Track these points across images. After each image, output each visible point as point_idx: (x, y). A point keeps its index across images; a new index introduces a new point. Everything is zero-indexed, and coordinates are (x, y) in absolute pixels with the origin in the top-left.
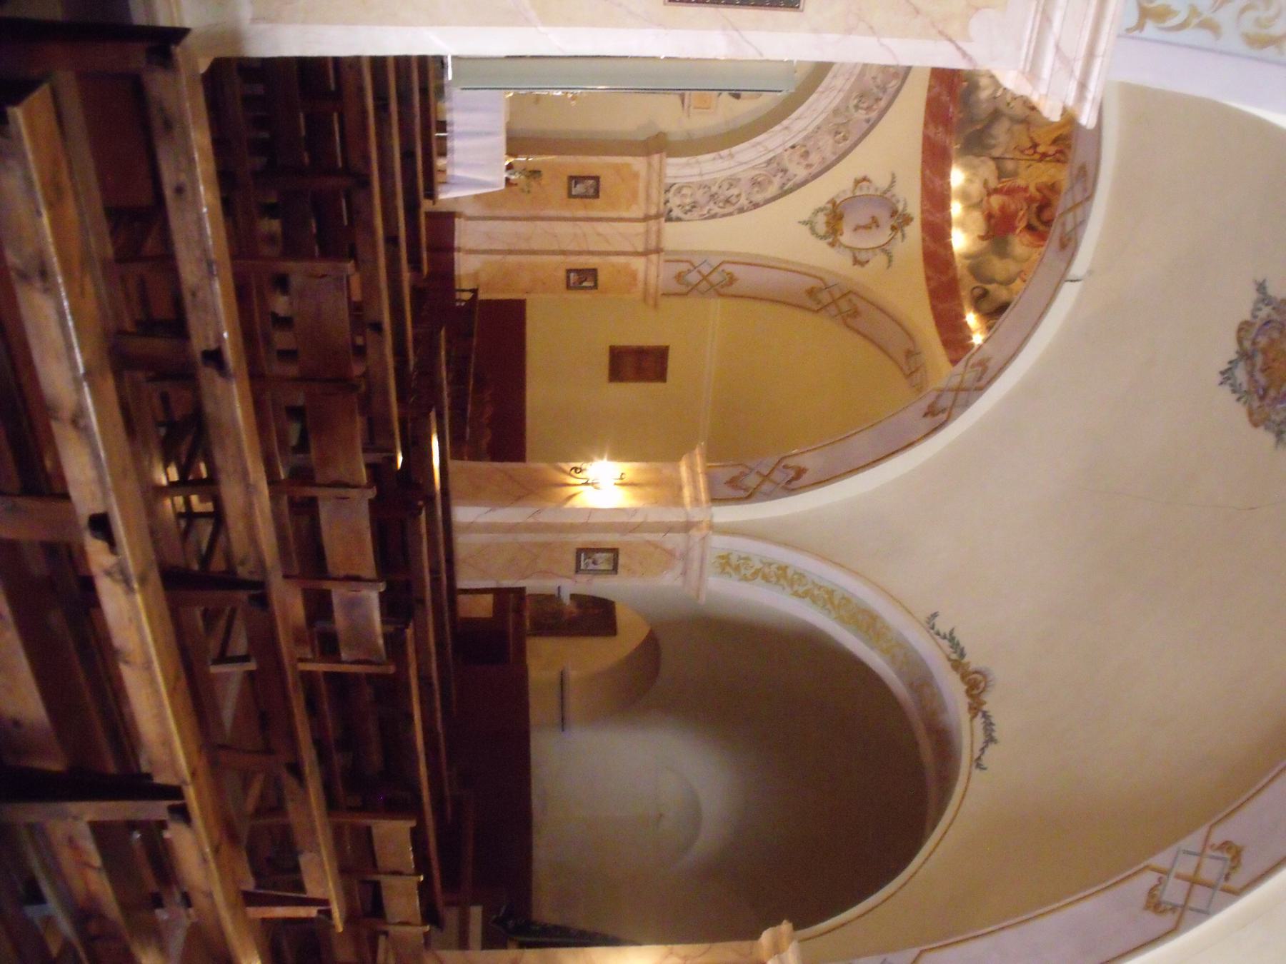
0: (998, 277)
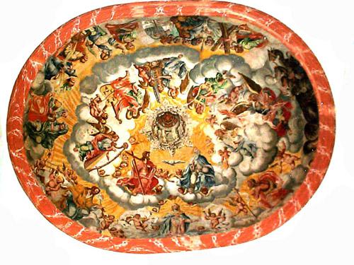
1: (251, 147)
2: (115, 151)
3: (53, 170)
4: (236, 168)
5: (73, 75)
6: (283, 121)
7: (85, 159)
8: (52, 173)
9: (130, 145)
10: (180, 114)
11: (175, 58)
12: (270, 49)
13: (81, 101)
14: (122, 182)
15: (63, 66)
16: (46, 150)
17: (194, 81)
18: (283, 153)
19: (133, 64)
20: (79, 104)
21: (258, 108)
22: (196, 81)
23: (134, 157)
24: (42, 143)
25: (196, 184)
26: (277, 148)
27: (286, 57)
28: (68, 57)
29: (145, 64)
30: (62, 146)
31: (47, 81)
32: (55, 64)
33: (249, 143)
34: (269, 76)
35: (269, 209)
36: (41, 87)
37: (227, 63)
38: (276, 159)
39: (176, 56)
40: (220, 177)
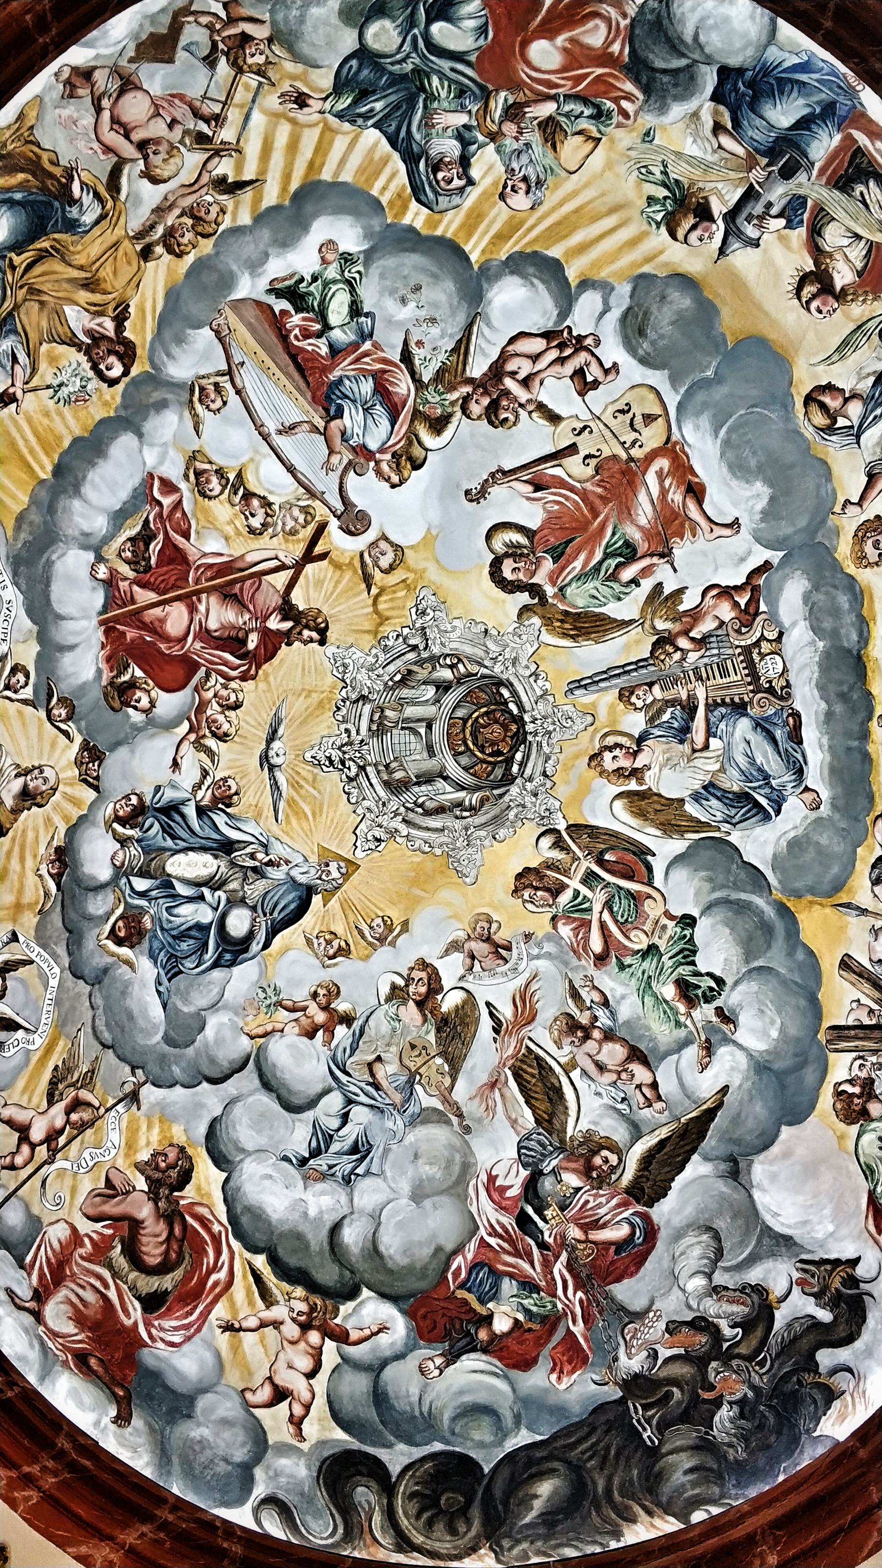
0: (240, 1455)
1: (354, 1149)
2: (328, 467)
3: (217, 120)
4: (248, 1079)
5: (732, 231)
6: (488, 1319)
7: (281, 305)
8: (197, 114)
9: (361, 543)
10: (514, 790)
11: (800, 773)
12: (861, 1271)
13: (585, 284)
14: (167, 501)
15: (787, 173)
16: (325, 80)
17: (679, 859)
18: (328, 1333)
19: (775, 557)
20: (572, 274)
21: (547, 1184)
22: (680, 874)
23: (299, 567)
24: (363, 54)
25: (167, 884)
26: (352, 1293)
27: (826, 1358)
28: (833, 199)
29: (773, 618)
30: (346, 177)
31: (709, 79)
32: (804, 124)
33: (378, 1141)
34: (719, 1253)
35: (24, 1292)
36: (675, 46)
37: (774, 1034)
38: (299, 1292)
39: (814, 777)
40: (200, 1000)
